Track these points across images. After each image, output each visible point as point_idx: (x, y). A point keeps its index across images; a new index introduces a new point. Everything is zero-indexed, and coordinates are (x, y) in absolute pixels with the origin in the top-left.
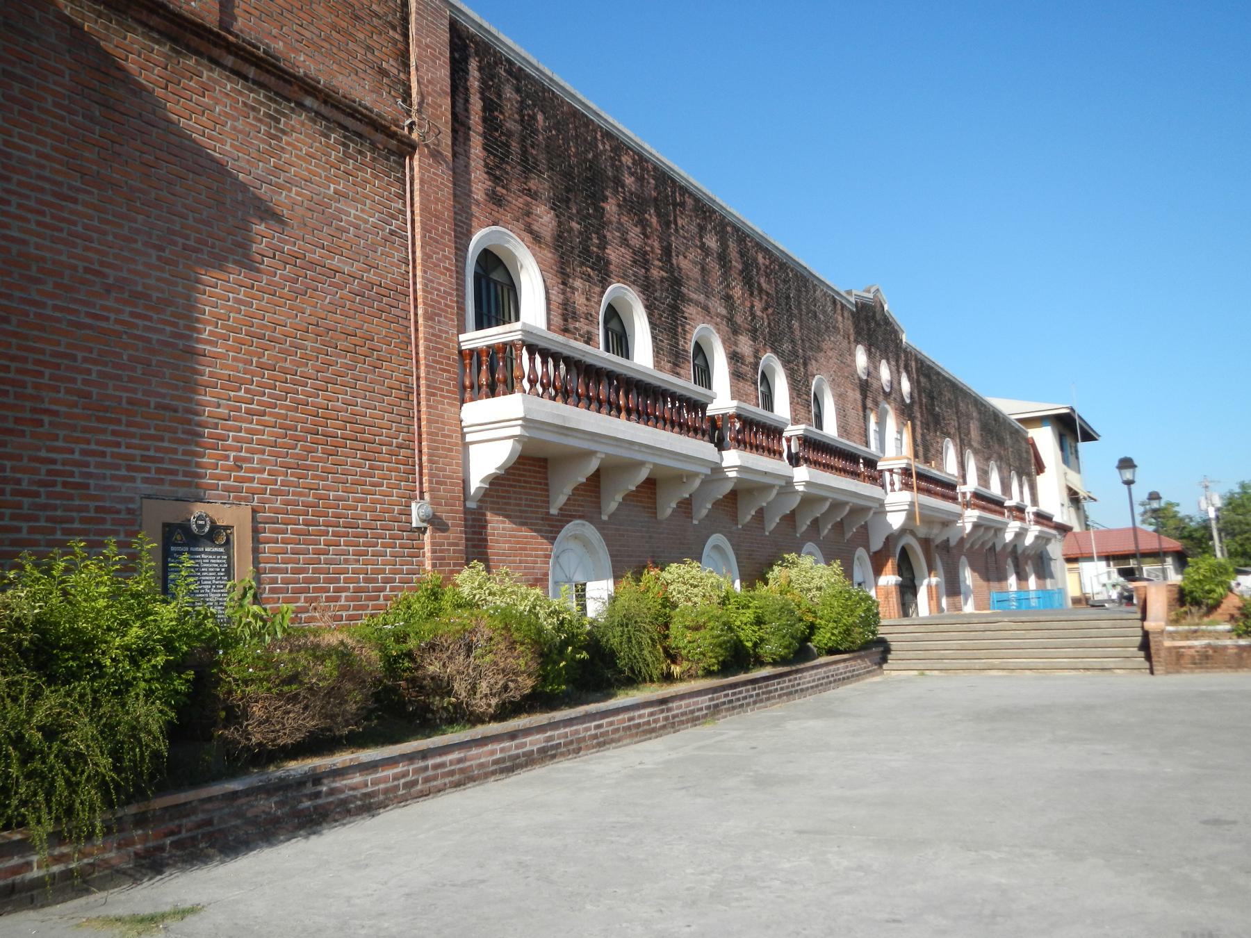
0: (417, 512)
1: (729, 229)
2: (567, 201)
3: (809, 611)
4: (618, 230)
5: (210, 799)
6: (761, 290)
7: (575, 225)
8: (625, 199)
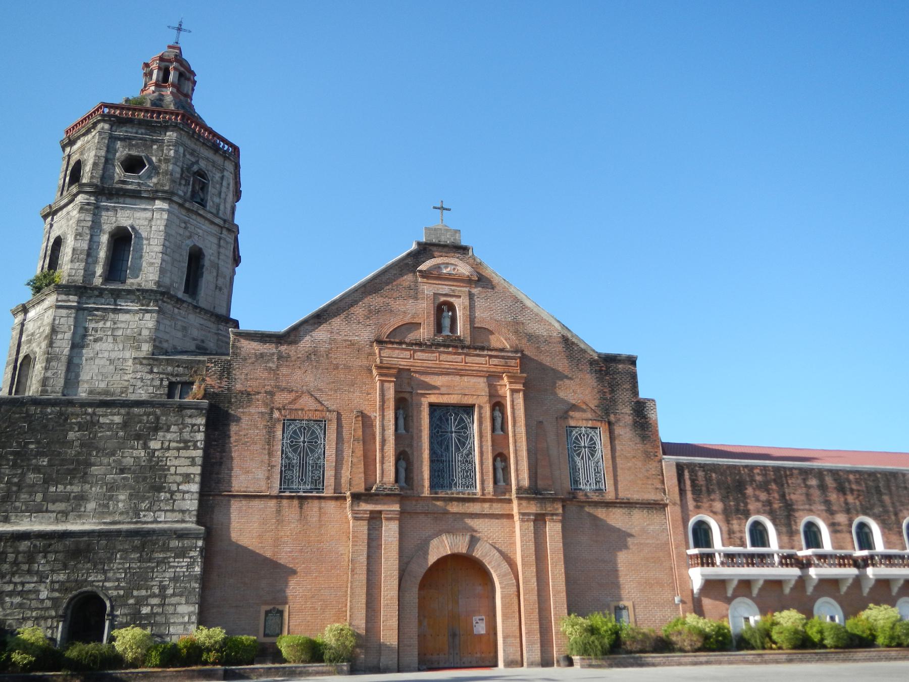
0: (677, 599)
1: (825, 473)
2: (728, 497)
3: (870, 630)
4: (754, 497)
5: (620, 658)
6: (852, 491)
7: (732, 503)
8: (757, 486)
